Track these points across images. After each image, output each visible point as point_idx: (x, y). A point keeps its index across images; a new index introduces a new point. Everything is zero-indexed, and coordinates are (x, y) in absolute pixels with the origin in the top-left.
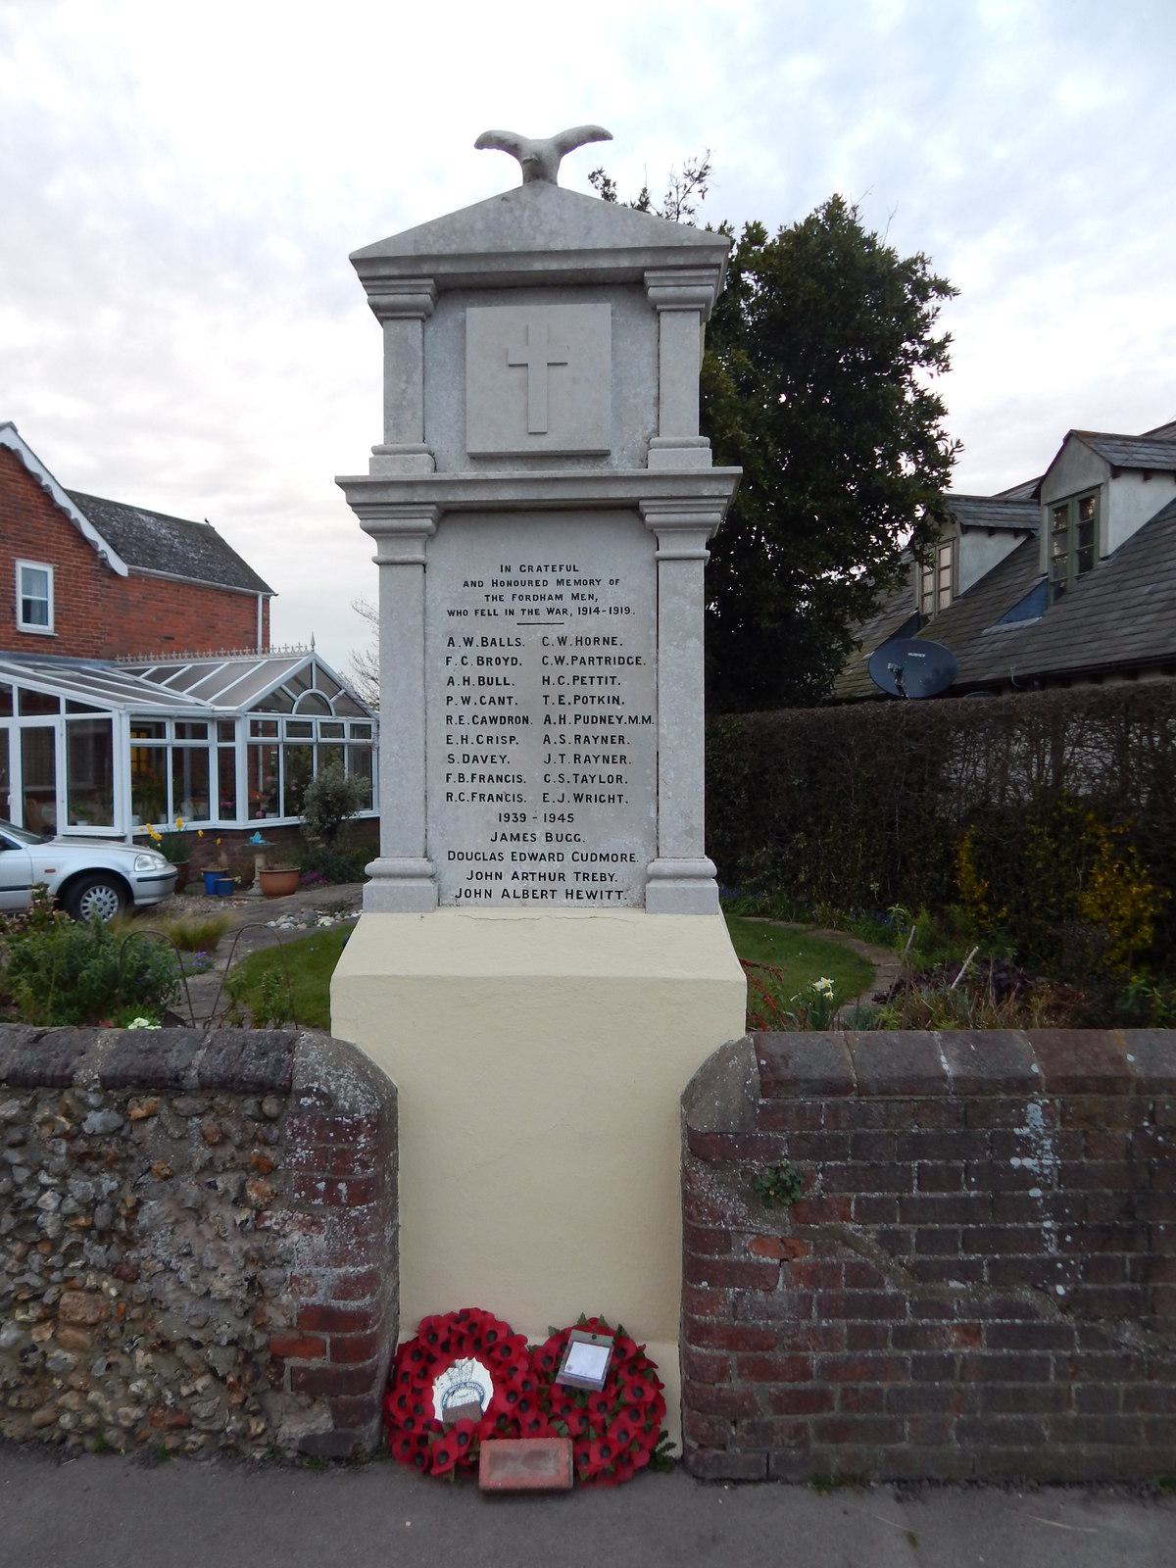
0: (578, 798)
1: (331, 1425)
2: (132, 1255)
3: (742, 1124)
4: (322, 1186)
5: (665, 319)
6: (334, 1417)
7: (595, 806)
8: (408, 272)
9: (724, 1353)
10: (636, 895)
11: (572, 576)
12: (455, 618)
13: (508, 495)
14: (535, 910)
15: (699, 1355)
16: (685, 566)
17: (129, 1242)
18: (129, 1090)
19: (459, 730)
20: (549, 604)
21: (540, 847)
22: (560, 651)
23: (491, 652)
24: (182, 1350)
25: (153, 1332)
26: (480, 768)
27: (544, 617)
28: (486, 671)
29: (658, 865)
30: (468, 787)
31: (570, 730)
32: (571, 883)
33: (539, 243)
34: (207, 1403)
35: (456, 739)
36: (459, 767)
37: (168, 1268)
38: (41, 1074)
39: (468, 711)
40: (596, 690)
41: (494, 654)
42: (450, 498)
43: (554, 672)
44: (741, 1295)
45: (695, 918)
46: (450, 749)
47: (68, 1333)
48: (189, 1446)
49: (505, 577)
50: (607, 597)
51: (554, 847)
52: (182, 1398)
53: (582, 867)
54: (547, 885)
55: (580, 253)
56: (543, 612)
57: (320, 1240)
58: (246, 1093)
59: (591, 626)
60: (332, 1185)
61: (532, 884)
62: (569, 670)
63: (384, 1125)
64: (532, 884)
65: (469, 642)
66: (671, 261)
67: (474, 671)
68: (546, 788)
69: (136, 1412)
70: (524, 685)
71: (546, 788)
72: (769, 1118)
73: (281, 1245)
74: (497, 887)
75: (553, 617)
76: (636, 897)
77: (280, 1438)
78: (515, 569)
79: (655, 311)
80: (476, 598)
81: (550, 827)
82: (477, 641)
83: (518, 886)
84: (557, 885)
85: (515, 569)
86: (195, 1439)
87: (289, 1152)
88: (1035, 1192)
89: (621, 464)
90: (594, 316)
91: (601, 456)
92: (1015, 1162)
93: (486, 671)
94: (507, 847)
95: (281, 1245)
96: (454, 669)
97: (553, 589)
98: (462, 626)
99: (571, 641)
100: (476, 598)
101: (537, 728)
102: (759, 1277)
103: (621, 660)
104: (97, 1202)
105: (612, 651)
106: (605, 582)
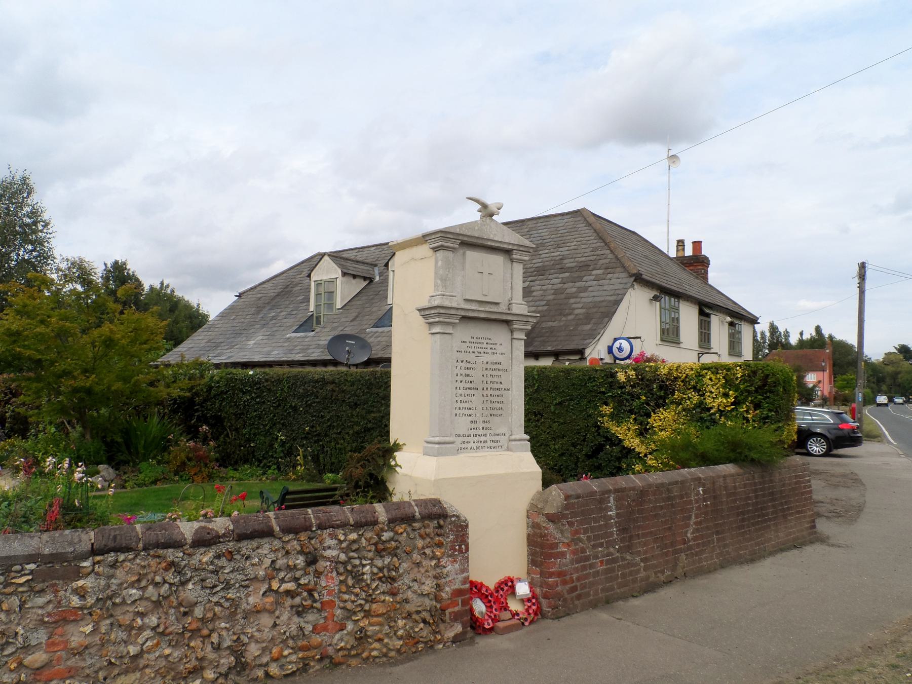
0: (491, 415)
1: (461, 629)
2: (396, 585)
3: (562, 510)
4: (457, 547)
5: (515, 264)
6: (462, 626)
7: (495, 417)
8: (455, 238)
9: (557, 579)
10: (505, 447)
11: (490, 342)
12: (459, 353)
13: (482, 315)
14: (480, 453)
15: (551, 581)
16: (520, 341)
17: (394, 579)
18: (396, 524)
19: (459, 392)
20: (484, 350)
21: (481, 432)
22: (485, 366)
23: (468, 365)
24: (415, 616)
25: (406, 611)
26: (465, 405)
27: (483, 355)
28: (467, 372)
29: (513, 437)
30: (462, 412)
31: (489, 392)
32: (489, 444)
33: (491, 237)
34: (425, 632)
35: (458, 395)
36: (459, 405)
37: (410, 587)
38: (366, 521)
39: (461, 385)
40: (496, 379)
41: (469, 366)
42: (467, 314)
43: (485, 373)
44: (560, 561)
45: (525, 453)
46: (457, 398)
47: (375, 619)
48: (420, 649)
49: (472, 340)
50: (499, 349)
51: (484, 432)
52: (416, 632)
53: (492, 438)
54: (482, 445)
55: (501, 242)
56: (482, 353)
57: (457, 566)
58: (435, 518)
59: (494, 358)
60: (460, 546)
61: (479, 445)
62: (489, 372)
63: (467, 526)
64: (479, 445)
65: (462, 362)
66: (521, 249)
67: (464, 372)
68: (483, 412)
69: (401, 643)
70: (477, 375)
71: (483, 412)
72: (567, 507)
73: (445, 571)
74: (469, 446)
75: (485, 355)
76: (506, 448)
77: (445, 639)
78: (475, 338)
79: (512, 261)
80: (464, 347)
81: (483, 425)
82: (465, 361)
83: (474, 445)
84: (485, 445)
85: (475, 338)
86: (421, 646)
87: (448, 537)
88: (612, 521)
89: (503, 308)
90: (498, 260)
91: (497, 304)
92: (609, 513)
93: (467, 372)
94: (472, 432)
95: (445, 571)
96: (458, 371)
97: (485, 346)
98: (461, 356)
99: (489, 363)
100: (464, 347)
101: (480, 392)
102: (563, 555)
103: (503, 370)
104: (384, 568)
105: (500, 367)
106: (498, 344)
